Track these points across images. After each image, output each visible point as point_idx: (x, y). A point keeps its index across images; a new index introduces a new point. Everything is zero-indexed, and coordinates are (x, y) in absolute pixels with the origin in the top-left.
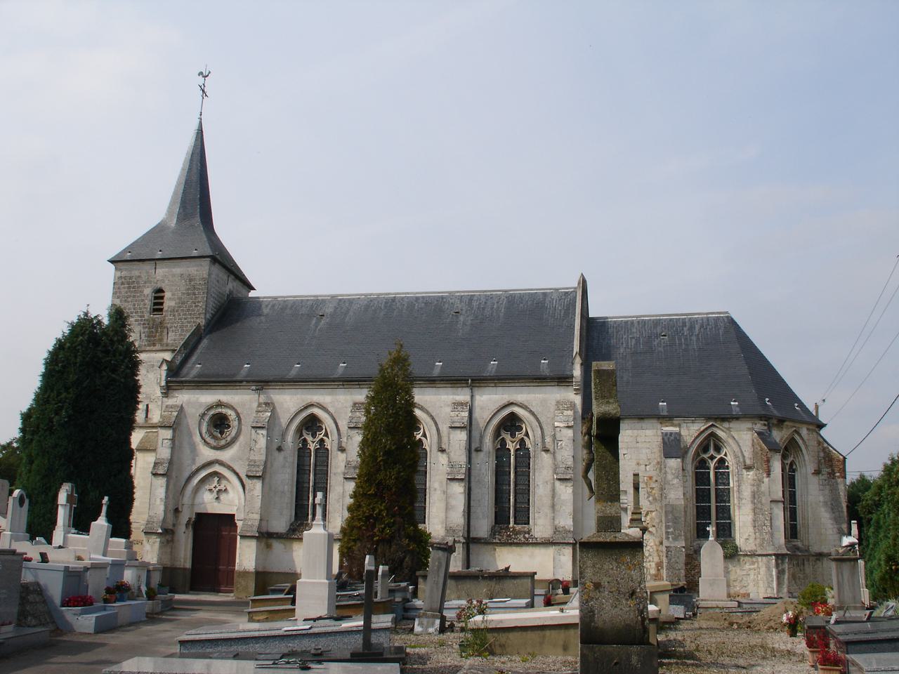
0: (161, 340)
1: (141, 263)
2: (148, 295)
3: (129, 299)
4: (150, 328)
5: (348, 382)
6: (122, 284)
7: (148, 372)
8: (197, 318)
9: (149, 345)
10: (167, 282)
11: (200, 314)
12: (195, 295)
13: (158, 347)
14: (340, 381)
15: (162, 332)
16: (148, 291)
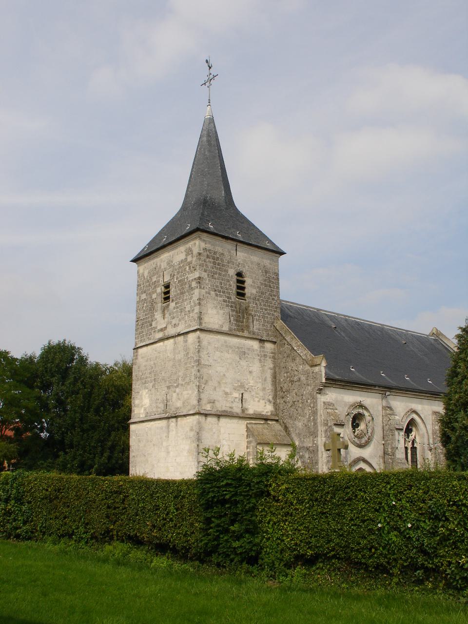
0: (248, 327)
1: (256, 249)
2: (232, 276)
3: (216, 276)
4: (237, 312)
5: (433, 395)
6: (208, 257)
7: (240, 359)
8: (275, 311)
9: (238, 330)
10: (247, 267)
11: (276, 308)
12: (271, 287)
13: (246, 334)
14: (429, 394)
15: (248, 318)
16: (232, 272)
